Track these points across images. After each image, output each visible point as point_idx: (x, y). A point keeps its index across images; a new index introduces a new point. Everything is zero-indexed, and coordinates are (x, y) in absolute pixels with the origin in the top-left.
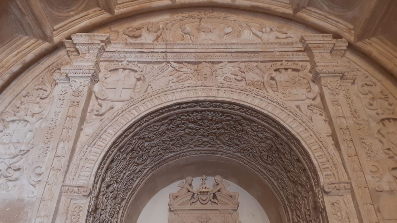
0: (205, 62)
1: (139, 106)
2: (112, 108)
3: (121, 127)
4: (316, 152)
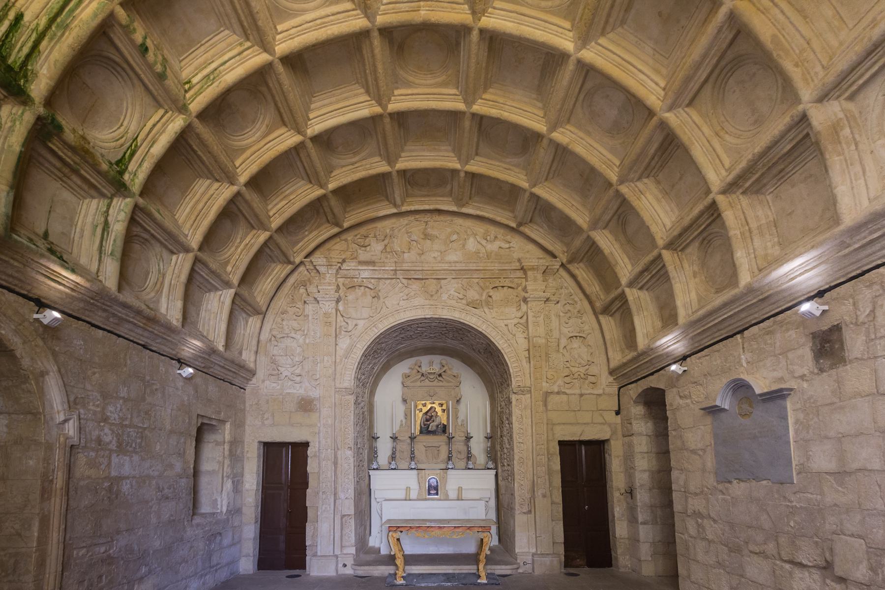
2: (356, 325)
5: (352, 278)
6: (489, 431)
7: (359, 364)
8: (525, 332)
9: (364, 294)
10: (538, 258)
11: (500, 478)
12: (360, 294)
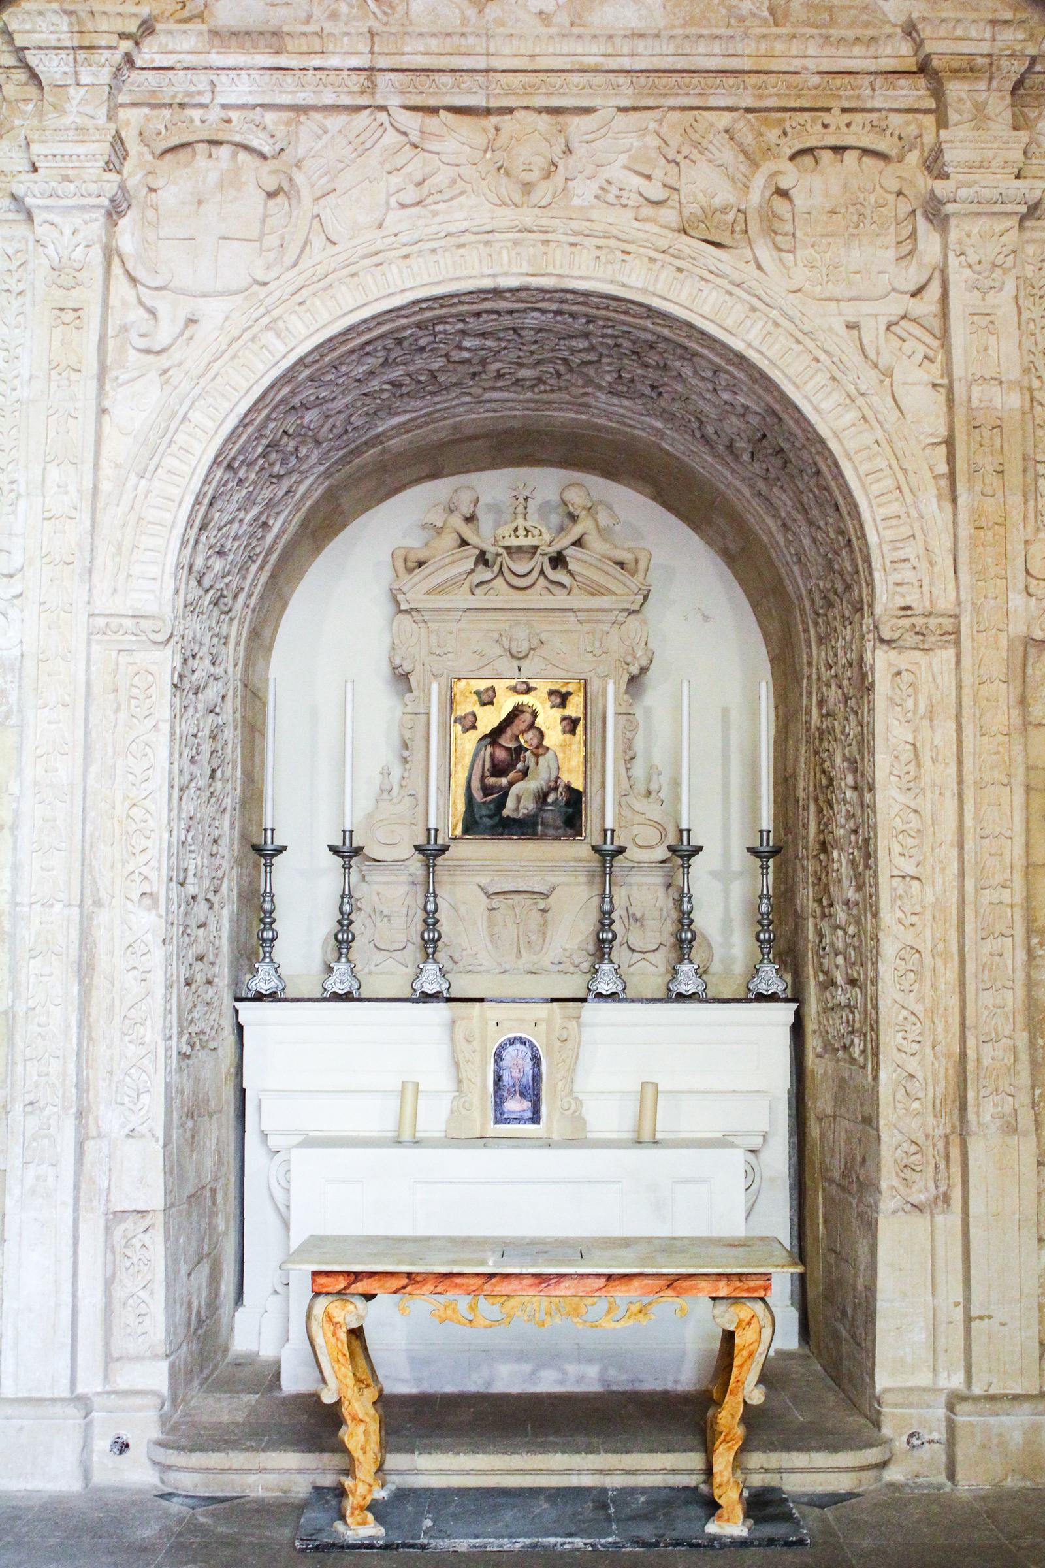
0: (527, 108)
1: (286, 316)
2: (191, 321)
3: (234, 401)
4: (879, 505)
5: (182, 105)
6: (766, 822)
7: (197, 502)
8: (931, 361)
9: (231, 181)
10: (993, 22)
11: (813, 1043)
12: (213, 177)
